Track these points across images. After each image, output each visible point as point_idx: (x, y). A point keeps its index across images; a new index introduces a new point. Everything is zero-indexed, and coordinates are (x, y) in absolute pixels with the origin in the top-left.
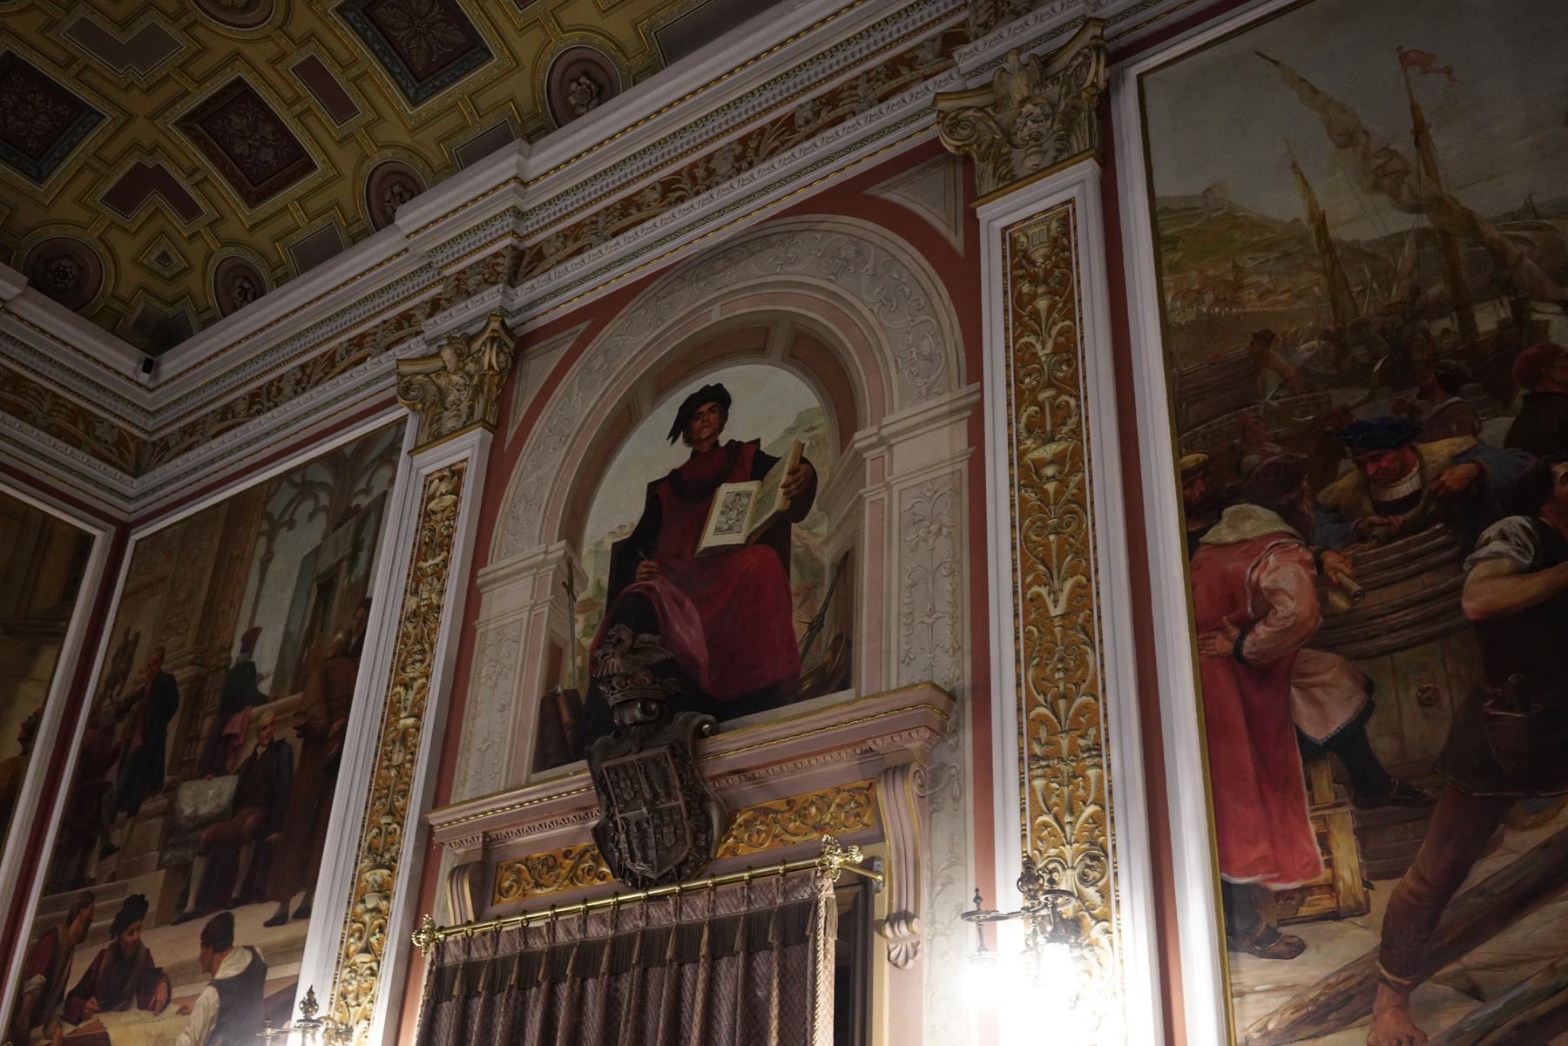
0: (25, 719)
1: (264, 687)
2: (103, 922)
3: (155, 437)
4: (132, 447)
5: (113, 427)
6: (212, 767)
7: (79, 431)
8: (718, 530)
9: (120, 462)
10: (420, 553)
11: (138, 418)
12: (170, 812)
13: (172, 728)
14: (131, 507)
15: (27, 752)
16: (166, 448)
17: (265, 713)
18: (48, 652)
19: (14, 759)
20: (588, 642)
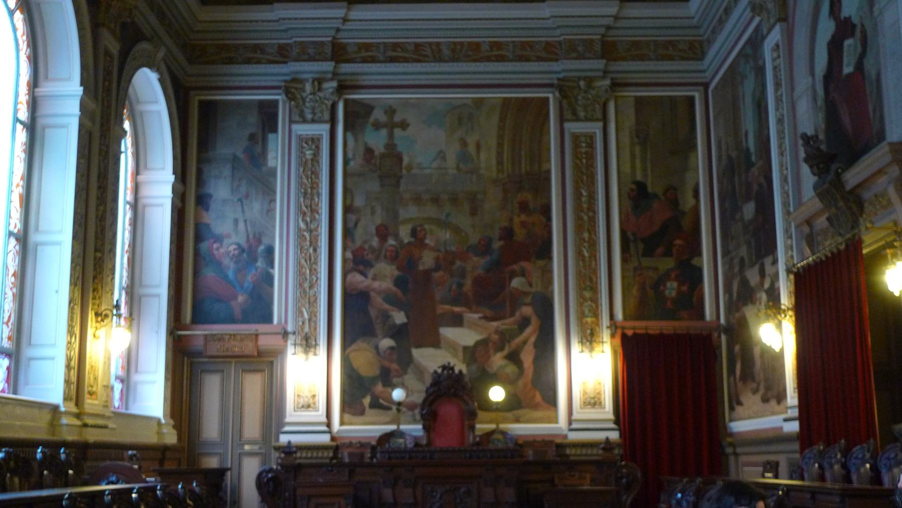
1: (753, 158)
2: (736, 269)
3: (705, 37)
5: (685, 41)
6: (748, 198)
8: (848, 66)
10: (776, 90)
12: (742, 219)
13: (736, 179)
17: (755, 170)
20: (823, 126)
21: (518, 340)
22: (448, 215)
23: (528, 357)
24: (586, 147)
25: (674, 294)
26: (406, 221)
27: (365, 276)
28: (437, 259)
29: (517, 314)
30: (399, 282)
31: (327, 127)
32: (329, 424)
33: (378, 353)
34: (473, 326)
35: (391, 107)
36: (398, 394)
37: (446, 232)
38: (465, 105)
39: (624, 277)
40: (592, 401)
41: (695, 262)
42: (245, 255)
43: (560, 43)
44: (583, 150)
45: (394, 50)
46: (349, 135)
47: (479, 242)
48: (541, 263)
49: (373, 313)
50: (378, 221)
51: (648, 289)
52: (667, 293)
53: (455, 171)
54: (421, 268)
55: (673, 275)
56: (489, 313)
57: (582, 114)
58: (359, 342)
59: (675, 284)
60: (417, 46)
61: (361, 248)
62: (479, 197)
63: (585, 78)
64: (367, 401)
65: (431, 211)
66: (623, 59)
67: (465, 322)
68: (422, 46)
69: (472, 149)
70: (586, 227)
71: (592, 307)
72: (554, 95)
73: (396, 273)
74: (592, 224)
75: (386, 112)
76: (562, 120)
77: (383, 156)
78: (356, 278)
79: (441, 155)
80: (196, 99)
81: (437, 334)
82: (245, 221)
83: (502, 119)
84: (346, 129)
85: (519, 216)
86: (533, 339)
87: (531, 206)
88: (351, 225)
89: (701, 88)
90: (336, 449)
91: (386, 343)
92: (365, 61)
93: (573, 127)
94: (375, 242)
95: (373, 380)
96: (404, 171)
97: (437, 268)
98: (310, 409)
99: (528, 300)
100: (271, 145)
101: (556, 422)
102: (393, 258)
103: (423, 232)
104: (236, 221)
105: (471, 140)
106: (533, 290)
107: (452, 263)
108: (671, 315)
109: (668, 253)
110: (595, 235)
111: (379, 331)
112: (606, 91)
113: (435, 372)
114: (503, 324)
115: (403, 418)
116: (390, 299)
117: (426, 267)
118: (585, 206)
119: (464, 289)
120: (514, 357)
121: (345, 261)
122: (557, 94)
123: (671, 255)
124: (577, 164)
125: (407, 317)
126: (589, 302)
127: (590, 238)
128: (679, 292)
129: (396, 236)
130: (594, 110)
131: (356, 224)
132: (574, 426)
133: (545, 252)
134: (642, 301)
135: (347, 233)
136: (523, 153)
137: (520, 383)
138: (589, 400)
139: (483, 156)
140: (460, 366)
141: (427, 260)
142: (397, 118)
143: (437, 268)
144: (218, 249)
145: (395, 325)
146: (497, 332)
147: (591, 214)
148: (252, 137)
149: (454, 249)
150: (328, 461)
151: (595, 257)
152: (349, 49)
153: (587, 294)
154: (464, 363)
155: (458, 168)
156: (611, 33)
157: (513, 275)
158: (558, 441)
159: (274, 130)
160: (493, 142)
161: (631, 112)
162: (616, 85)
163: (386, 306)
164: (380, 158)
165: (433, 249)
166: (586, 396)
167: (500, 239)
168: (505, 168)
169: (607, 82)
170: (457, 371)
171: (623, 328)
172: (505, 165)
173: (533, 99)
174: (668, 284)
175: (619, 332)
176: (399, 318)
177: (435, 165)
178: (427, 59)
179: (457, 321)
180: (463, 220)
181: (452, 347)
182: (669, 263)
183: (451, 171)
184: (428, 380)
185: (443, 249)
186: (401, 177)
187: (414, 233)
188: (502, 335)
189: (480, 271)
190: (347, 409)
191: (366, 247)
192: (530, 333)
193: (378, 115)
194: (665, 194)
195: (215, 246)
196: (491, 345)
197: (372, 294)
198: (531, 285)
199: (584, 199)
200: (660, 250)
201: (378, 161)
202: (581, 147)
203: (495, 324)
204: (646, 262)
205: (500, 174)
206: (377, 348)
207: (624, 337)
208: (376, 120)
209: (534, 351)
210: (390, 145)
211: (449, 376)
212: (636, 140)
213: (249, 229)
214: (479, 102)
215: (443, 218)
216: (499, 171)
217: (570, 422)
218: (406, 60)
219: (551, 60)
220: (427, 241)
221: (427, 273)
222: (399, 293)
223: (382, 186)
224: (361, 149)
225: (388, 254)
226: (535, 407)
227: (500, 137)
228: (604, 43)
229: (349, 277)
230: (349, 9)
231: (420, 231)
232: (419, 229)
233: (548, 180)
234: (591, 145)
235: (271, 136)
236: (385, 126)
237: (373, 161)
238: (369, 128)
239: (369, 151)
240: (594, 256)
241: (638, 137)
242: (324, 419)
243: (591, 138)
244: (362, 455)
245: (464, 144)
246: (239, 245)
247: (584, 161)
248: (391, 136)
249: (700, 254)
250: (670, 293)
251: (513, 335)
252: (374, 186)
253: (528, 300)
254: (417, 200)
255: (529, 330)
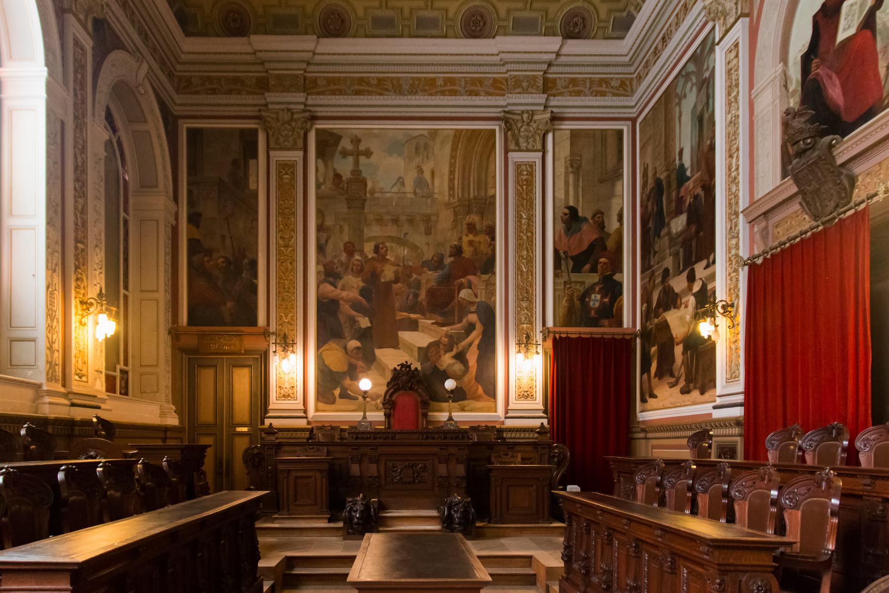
0: (617, 213)
4: (628, 83)
5: (617, 79)
7: (604, 88)
9: (625, 93)
11: (626, 70)
14: (634, 110)
15: (622, 224)
16: (640, 78)
18: (618, 184)
19: (617, 229)
21: (464, 343)
22: (405, 234)
23: (472, 358)
24: (527, 175)
25: (597, 304)
26: (370, 239)
27: (336, 287)
28: (396, 273)
29: (464, 321)
30: (363, 292)
31: (301, 153)
32: (305, 411)
33: (347, 353)
34: (427, 330)
35: (356, 136)
36: (365, 384)
37: (404, 249)
38: (422, 135)
39: (555, 290)
40: (526, 394)
41: (617, 277)
42: (232, 268)
43: (506, 80)
44: (524, 177)
45: (358, 85)
46: (320, 161)
47: (432, 258)
48: (485, 277)
49: (342, 318)
50: (346, 239)
51: (575, 300)
52: (591, 303)
53: (413, 196)
54: (383, 280)
55: (597, 289)
56: (440, 319)
57: (523, 145)
58: (330, 342)
59: (599, 297)
60: (378, 79)
61: (331, 262)
62: (433, 218)
63: (527, 111)
64: (337, 392)
65: (391, 230)
66: (561, 94)
67: (420, 328)
68: (385, 80)
69: (427, 175)
70: (525, 246)
71: (528, 315)
72: (500, 126)
73: (362, 284)
74: (530, 243)
75: (352, 141)
76: (506, 151)
77: (349, 181)
78: (328, 288)
79: (401, 181)
80: (184, 126)
81: (397, 337)
82: (231, 238)
83: (454, 149)
84: (317, 157)
85: (467, 235)
86: (477, 342)
87: (478, 226)
88: (323, 242)
89: (629, 123)
90: (311, 430)
91: (354, 344)
92: (333, 93)
93: (515, 157)
94: (344, 257)
95: (342, 375)
96: (368, 195)
97: (396, 281)
98: (289, 398)
99: (473, 309)
100: (252, 171)
101: (496, 411)
102: (359, 271)
103: (385, 249)
104: (223, 237)
105: (427, 168)
106: (478, 300)
107: (410, 276)
108: (594, 323)
109: (594, 270)
110: (533, 254)
111: (347, 334)
112: (547, 123)
113: (395, 369)
114: (451, 330)
115: (368, 407)
116: (356, 306)
117: (388, 279)
118: (525, 227)
119: (419, 299)
120: (461, 357)
121: (318, 273)
122: (503, 125)
123: (597, 272)
124: (518, 190)
125: (371, 322)
126: (526, 311)
127: (528, 255)
128: (602, 304)
129: (362, 252)
130: (535, 141)
131: (327, 241)
132: (509, 415)
133: (488, 266)
134: (570, 311)
135: (320, 249)
136: (472, 179)
137: (466, 379)
138: (523, 393)
139: (437, 182)
140: (416, 365)
141: (388, 273)
142: (362, 147)
143: (396, 281)
144: (208, 261)
145: (360, 328)
146: (447, 335)
147: (529, 234)
148: (235, 162)
149: (411, 264)
150: (305, 441)
151: (532, 272)
152: (319, 82)
153: (524, 304)
154: (419, 361)
155: (415, 193)
156: (553, 69)
157: (461, 287)
158: (498, 426)
159: (255, 156)
160: (446, 170)
161: (567, 144)
162: (555, 118)
163: (354, 313)
164: (347, 183)
165: (393, 264)
166: (521, 390)
167: (450, 256)
168: (456, 193)
169: (548, 115)
170: (413, 368)
171: (555, 333)
172: (456, 191)
173: (481, 130)
174: (593, 296)
175: (551, 336)
176: (364, 322)
177: (395, 189)
178: (388, 93)
179: (413, 326)
180: (419, 239)
181: (409, 348)
182: (594, 278)
183: (409, 196)
184: (389, 376)
185: (401, 264)
186: (366, 200)
187: (377, 249)
188: (450, 336)
189: (433, 283)
190: (320, 398)
191: (336, 261)
192: (475, 336)
193: (346, 144)
194: (593, 217)
195: (206, 259)
196: (441, 346)
197: (341, 302)
198: (476, 296)
199: (523, 221)
200: (587, 267)
201: (346, 185)
202: (523, 175)
203: (445, 329)
204: (575, 277)
205: (451, 199)
206: (345, 348)
207: (556, 342)
208: (344, 148)
209: (478, 351)
210: (356, 172)
211: (408, 372)
212: (570, 169)
213: (234, 244)
214: (434, 133)
215: (402, 237)
216: (450, 195)
217: (507, 411)
218: (370, 93)
219: (498, 95)
220: (388, 257)
221: (388, 284)
222: (364, 301)
223: (348, 208)
224: (331, 175)
225: (355, 267)
226: (477, 398)
227: (452, 165)
228: (546, 81)
229: (321, 287)
230: (318, 43)
231: (382, 248)
232: (381, 246)
233: (494, 204)
234: (531, 174)
235: (252, 162)
236: (351, 154)
237: (341, 186)
238: (337, 156)
239: (338, 176)
240: (531, 272)
241: (572, 166)
242: (302, 407)
243: (532, 166)
244: (333, 436)
245: (420, 171)
246: (225, 257)
247: (525, 187)
248: (357, 163)
249: (621, 271)
250: (594, 304)
251: (461, 338)
252: (342, 207)
253: (473, 309)
254: (380, 221)
255: (474, 334)
